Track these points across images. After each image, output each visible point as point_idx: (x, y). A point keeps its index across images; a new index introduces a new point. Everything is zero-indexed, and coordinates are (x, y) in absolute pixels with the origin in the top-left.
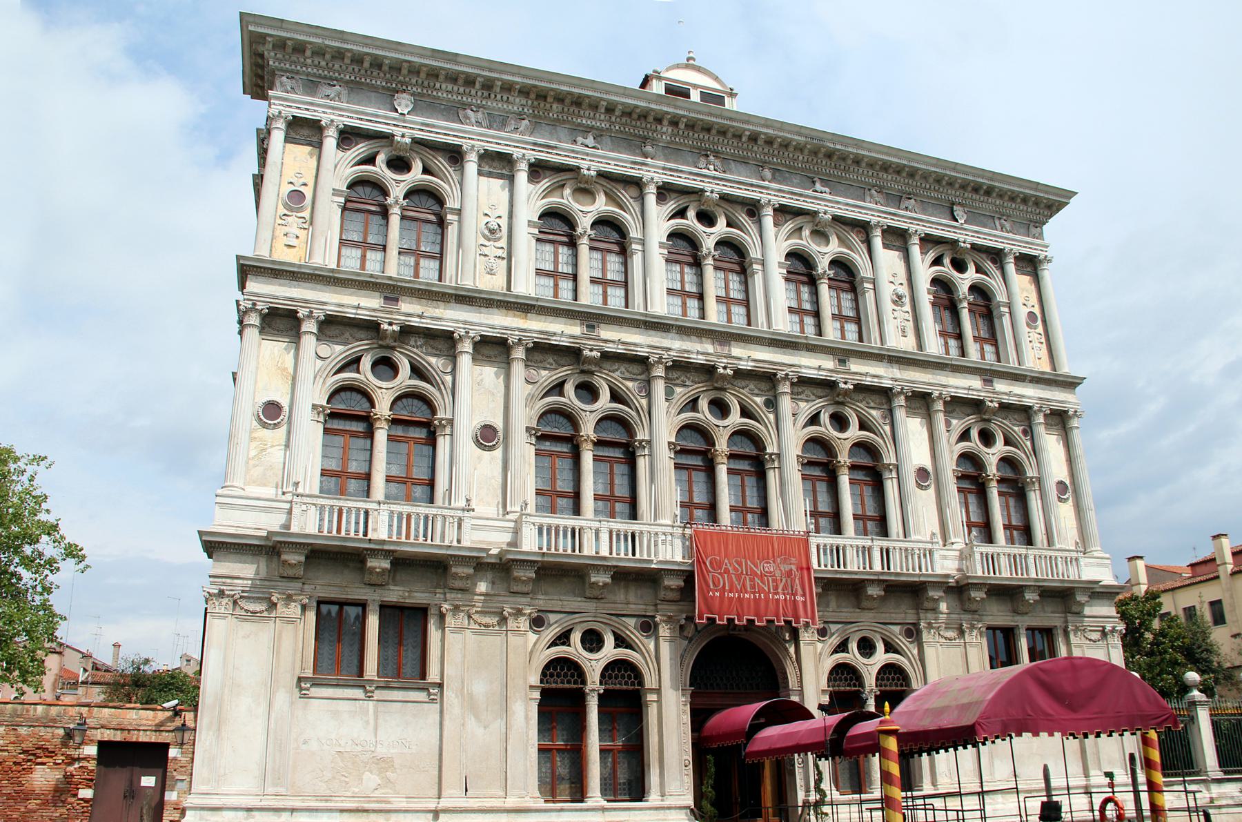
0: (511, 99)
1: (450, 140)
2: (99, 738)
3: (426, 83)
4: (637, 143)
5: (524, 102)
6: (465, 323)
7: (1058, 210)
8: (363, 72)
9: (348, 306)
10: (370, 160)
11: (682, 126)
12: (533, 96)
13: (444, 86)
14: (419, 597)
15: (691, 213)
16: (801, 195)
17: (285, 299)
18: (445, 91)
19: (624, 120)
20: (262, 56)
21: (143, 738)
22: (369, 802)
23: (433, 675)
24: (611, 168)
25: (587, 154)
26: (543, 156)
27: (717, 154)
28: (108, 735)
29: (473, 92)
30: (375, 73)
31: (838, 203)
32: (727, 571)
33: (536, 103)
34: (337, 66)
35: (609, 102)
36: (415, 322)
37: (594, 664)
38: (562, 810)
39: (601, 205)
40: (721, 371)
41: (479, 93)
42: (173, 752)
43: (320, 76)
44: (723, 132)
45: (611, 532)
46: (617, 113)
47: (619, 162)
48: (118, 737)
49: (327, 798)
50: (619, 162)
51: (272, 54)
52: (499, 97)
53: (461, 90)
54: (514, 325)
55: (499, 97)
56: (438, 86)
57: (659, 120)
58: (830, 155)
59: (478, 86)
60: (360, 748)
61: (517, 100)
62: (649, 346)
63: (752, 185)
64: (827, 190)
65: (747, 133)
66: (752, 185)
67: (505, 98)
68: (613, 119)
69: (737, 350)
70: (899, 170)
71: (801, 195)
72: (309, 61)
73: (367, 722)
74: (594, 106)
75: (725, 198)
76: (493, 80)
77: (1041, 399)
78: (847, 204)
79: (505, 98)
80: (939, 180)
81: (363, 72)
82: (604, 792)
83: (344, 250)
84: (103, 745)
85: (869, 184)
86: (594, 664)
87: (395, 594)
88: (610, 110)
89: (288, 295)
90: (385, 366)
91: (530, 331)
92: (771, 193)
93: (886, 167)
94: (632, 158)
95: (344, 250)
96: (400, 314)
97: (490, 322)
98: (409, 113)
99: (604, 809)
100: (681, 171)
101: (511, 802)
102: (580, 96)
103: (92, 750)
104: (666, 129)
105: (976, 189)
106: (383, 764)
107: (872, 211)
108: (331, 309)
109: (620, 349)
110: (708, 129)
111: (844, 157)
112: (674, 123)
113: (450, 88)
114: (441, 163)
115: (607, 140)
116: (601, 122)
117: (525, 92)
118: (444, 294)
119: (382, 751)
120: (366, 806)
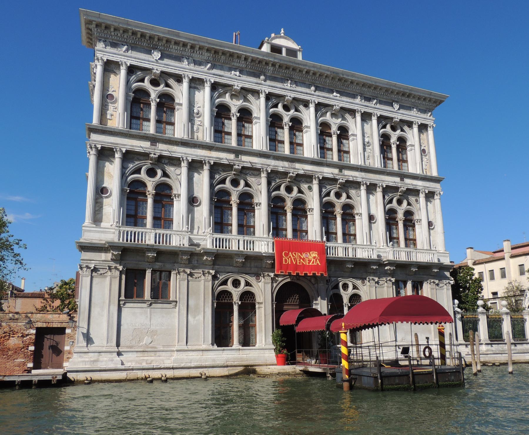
0: (203, 53)
1: (177, 72)
2: (36, 326)
3: (166, 45)
5: (209, 55)
6: (185, 154)
7: (440, 104)
8: (137, 39)
9: (136, 146)
10: (142, 80)
11: (277, 67)
12: (213, 52)
13: (173, 47)
14: (168, 266)
15: (280, 106)
16: (327, 98)
17: (108, 143)
18: (174, 50)
19: (252, 64)
20: (91, 30)
21: (55, 325)
22: (148, 348)
24: (247, 86)
25: (237, 79)
26: (218, 80)
27: (291, 79)
28: (39, 325)
29: (187, 50)
30: (143, 40)
31: (343, 101)
32: (290, 257)
33: (214, 56)
34: (125, 37)
35: (246, 56)
36: (165, 153)
37: (236, 293)
38: (224, 350)
41: (189, 51)
42: (68, 331)
43: (118, 41)
44: (294, 69)
45: (244, 241)
46: (249, 60)
48: (44, 325)
49: (131, 347)
50: (249, 82)
51: (96, 29)
52: (198, 53)
53: (181, 49)
54: (206, 155)
55: (198, 53)
56: (171, 47)
57: (267, 64)
58: (340, 80)
59: (189, 47)
60: (144, 327)
61: (206, 54)
62: (261, 164)
63: (307, 93)
64: (338, 95)
65: (306, 70)
66: (307, 93)
67: (201, 53)
68: (248, 63)
69: (298, 165)
70: (370, 86)
71: (327, 98)
72: (113, 34)
73: (147, 317)
74: (239, 57)
75: (294, 99)
76: (195, 45)
77: (424, 187)
78: (347, 102)
79: (201, 53)
80: (387, 90)
81: (137, 39)
82: (240, 343)
83: (132, 120)
84: (38, 329)
85: (357, 92)
86: (236, 293)
87: (158, 266)
88: (246, 59)
89: (109, 141)
90: (151, 173)
91: (212, 157)
92: (315, 96)
93: (364, 85)
95: (132, 120)
96: (158, 150)
97: (196, 153)
98: (159, 59)
99: (239, 350)
100: (277, 87)
101: (204, 347)
102: (233, 53)
103: (34, 332)
104: (271, 68)
105: (404, 95)
106: (154, 333)
107: (358, 104)
108: (129, 148)
109: (249, 165)
110: (287, 68)
111: (346, 81)
112: (274, 65)
113: (176, 48)
114: (171, 82)
116: (242, 64)
117: (208, 50)
118: (176, 142)
119: (153, 328)
120: (147, 350)
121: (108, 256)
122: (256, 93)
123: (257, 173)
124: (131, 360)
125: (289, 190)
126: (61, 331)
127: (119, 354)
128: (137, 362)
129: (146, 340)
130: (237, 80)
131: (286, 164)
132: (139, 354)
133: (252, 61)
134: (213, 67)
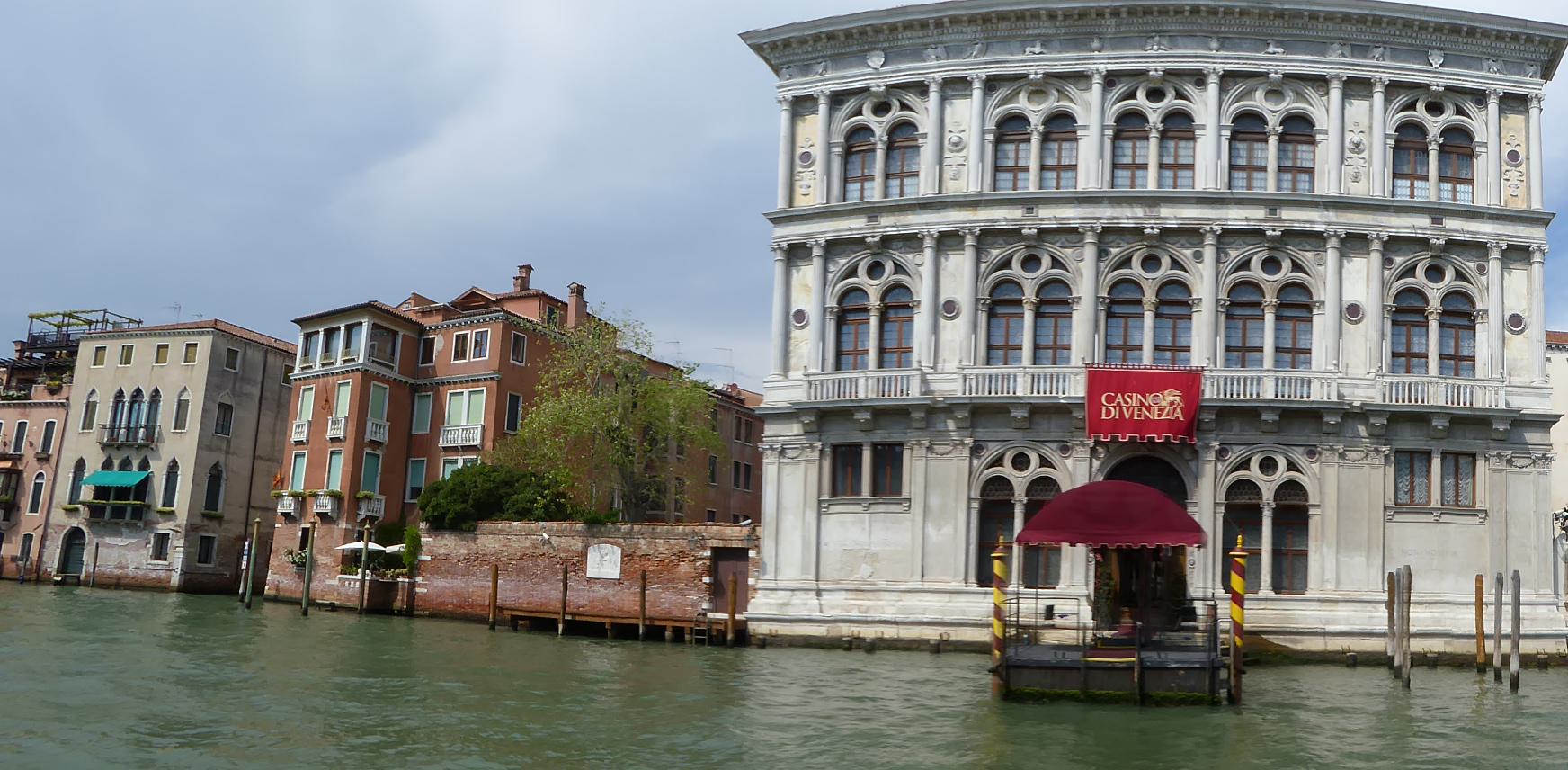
4: (1078, 41)
21: (735, 545)
23: (905, 495)
24: (1059, 69)
28: (715, 543)
39: (1052, 103)
40: (1148, 231)
42: (752, 554)
47: (1063, 61)
49: (838, 582)
50: (1063, 61)
84: (714, 549)
94: (1075, 55)
106: (873, 558)
115: (1056, 44)
119: (874, 549)
121: (796, 428)
122: (1081, 78)
123: (1074, 237)
124: (837, 604)
125: (1151, 262)
126: (741, 554)
127: (819, 593)
128: (843, 608)
129: (865, 570)
130: (1036, 62)
131: (1139, 211)
132: (850, 595)
133: (1066, 17)
134: (984, 52)
